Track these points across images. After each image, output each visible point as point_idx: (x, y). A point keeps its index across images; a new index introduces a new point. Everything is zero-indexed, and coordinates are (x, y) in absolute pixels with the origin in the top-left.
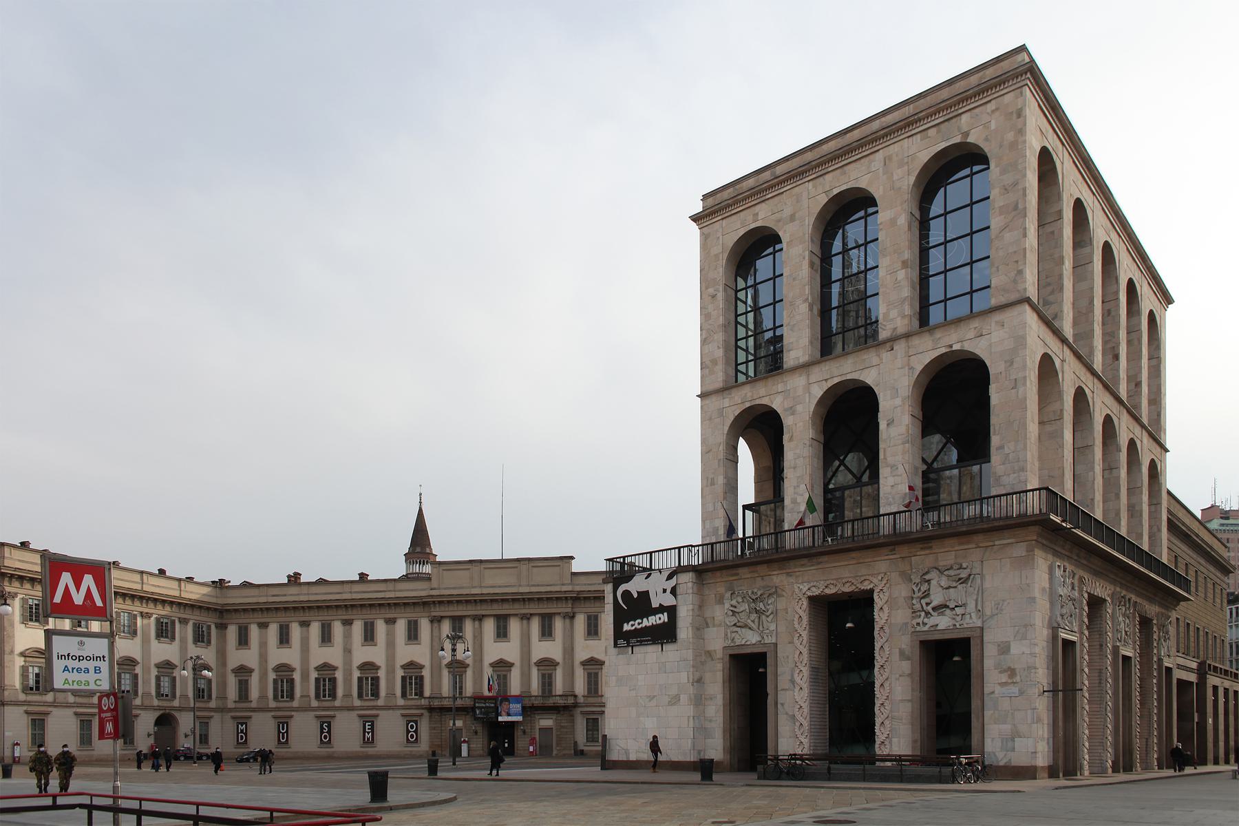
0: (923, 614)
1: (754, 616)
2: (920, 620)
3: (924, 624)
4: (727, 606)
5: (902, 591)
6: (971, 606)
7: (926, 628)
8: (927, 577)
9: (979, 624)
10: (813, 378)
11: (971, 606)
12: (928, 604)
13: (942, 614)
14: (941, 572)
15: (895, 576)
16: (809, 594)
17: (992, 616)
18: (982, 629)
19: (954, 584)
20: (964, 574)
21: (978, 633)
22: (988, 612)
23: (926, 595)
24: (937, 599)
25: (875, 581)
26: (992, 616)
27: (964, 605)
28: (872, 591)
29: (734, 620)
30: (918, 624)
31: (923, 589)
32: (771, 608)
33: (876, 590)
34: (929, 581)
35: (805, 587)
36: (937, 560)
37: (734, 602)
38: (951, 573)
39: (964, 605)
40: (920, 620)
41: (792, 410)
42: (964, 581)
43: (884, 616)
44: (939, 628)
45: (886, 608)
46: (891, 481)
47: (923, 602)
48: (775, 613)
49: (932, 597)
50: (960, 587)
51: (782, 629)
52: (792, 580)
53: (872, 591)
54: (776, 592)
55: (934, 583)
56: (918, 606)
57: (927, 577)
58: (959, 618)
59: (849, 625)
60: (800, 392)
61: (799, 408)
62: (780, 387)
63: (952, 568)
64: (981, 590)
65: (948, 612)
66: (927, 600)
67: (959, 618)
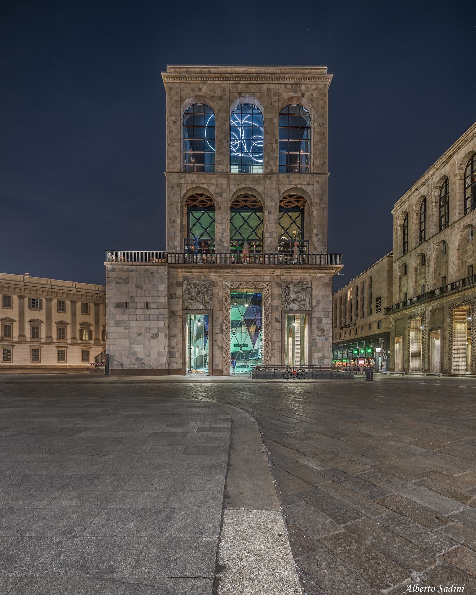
2: (285, 305)
3: (287, 307)
6: (307, 300)
7: (288, 309)
8: (289, 286)
12: (289, 298)
20: (305, 287)
23: (289, 295)
24: (293, 296)
25: (265, 285)
29: (188, 296)
36: (292, 279)
37: (189, 287)
38: (300, 285)
40: (285, 305)
41: (220, 195)
46: (270, 240)
48: (213, 295)
49: (291, 295)
51: (216, 302)
52: (221, 279)
55: (291, 289)
56: (284, 299)
60: (224, 186)
64: (311, 295)
65: (297, 303)
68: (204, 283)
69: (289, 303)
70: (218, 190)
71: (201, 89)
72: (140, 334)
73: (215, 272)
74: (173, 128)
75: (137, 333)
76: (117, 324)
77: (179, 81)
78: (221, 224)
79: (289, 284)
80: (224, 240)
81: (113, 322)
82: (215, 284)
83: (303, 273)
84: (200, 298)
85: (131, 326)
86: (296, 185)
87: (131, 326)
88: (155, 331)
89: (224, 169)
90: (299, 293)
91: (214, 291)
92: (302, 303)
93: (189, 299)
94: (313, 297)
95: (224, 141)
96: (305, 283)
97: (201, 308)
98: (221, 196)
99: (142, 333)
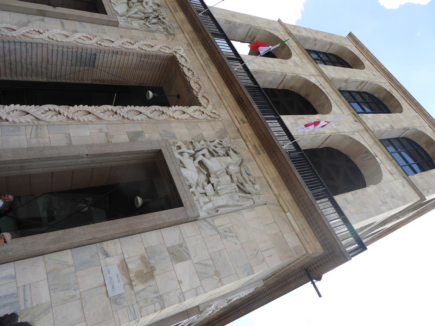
0: (192, 152)
2: (184, 149)
3: (181, 154)
5: (208, 131)
8: (231, 152)
9: (202, 214)
10: (318, 78)
12: (204, 155)
13: (199, 171)
14: (240, 165)
15: (219, 126)
16: (178, 56)
17: (215, 228)
18: (195, 219)
19: (235, 179)
20: (248, 187)
21: (191, 215)
22: (218, 222)
24: (213, 164)
25: (210, 107)
26: (215, 228)
27: (217, 193)
28: (200, 104)
30: (179, 148)
31: (217, 150)
32: (154, 27)
33: (202, 109)
34: (228, 155)
35: (182, 52)
36: (250, 161)
39: (217, 193)
42: (241, 189)
43: (178, 115)
45: (184, 116)
47: (205, 151)
49: (214, 159)
50: (234, 186)
53: (200, 104)
54: (169, 33)
57: (231, 152)
58: (200, 189)
59: (151, 93)
63: (249, 175)
64: (238, 209)
65: (203, 178)
66: (208, 154)
67: (200, 189)
69: (193, 157)
73: (192, 39)
79: (235, 152)
83: (274, 180)
84: (136, 13)
86: (377, 156)
90: (228, 178)
91: (157, 35)
92: (209, 188)
94: (235, 214)
96: (257, 186)
97: (116, 9)
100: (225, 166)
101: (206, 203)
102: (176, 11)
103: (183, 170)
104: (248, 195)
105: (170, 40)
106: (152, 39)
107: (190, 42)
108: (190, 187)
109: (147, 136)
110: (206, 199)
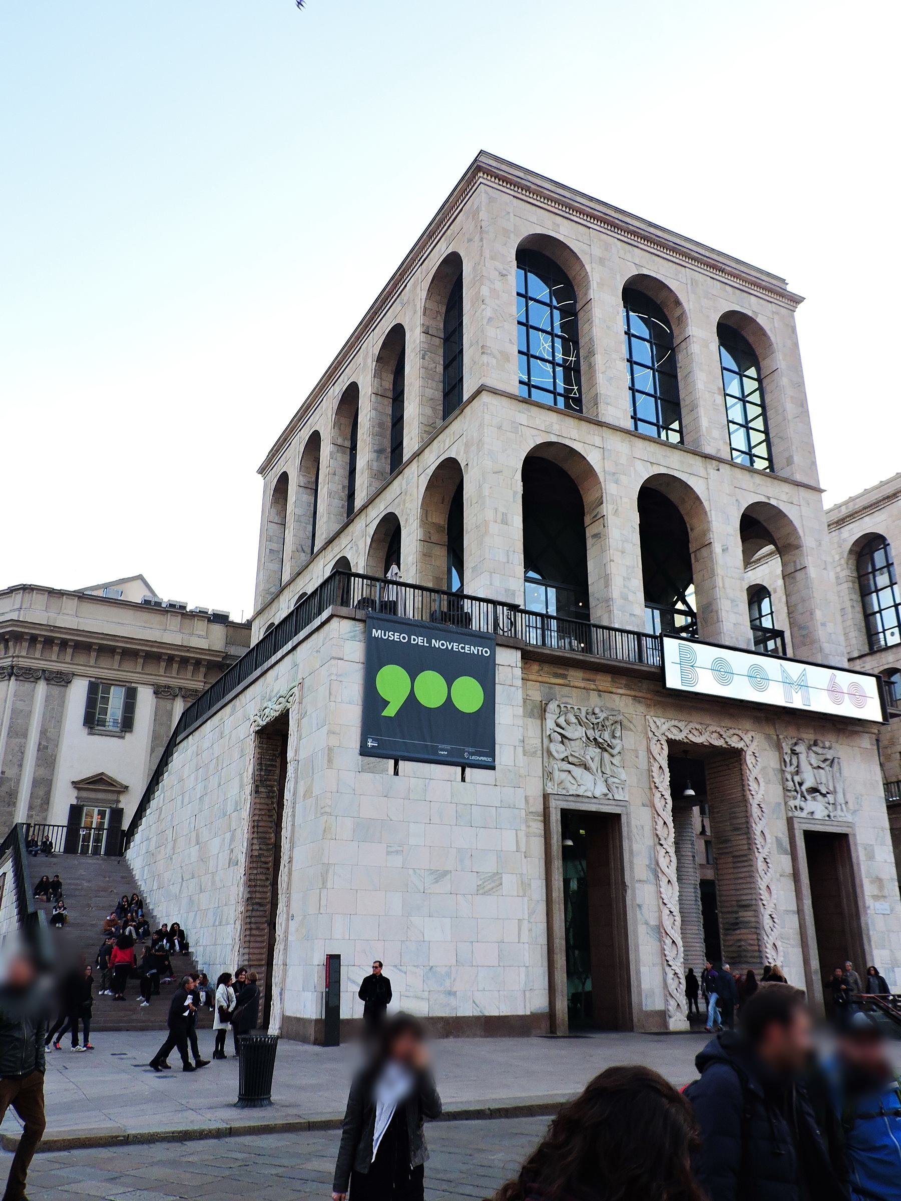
1: (594, 751)
3: (802, 809)
4: (550, 724)
7: (804, 814)
11: (840, 797)
12: (801, 784)
17: (855, 811)
19: (823, 765)
25: (745, 738)
26: (855, 811)
37: (561, 721)
44: (817, 816)
47: (797, 779)
55: (803, 757)
56: (790, 784)
60: (623, 460)
61: (623, 478)
62: (597, 441)
65: (820, 797)
67: (831, 807)
68: (602, 716)
70: (610, 466)
71: (558, 226)
72: (440, 875)
74: (498, 285)
75: (432, 872)
76: (366, 831)
77: (512, 193)
78: (623, 552)
80: (631, 597)
81: (349, 822)
82: (625, 722)
85: (412, 841)
87: (412, 841)
88: (489, 866)
89: (619, 419)
90: (821, 771)
93: (563, 760)
95: (614, 356)
98: (617, 482)
99: (446, 873)
100: (810, 767)
101: (842, 810)
102: (564, 677)
103: (817, 816)
104: (836, 760)
105: (632, 726)
106: (637, 757)
107: (633, 693)
108: (829, 816)
109: (780, 835)
110: (839, 807)
